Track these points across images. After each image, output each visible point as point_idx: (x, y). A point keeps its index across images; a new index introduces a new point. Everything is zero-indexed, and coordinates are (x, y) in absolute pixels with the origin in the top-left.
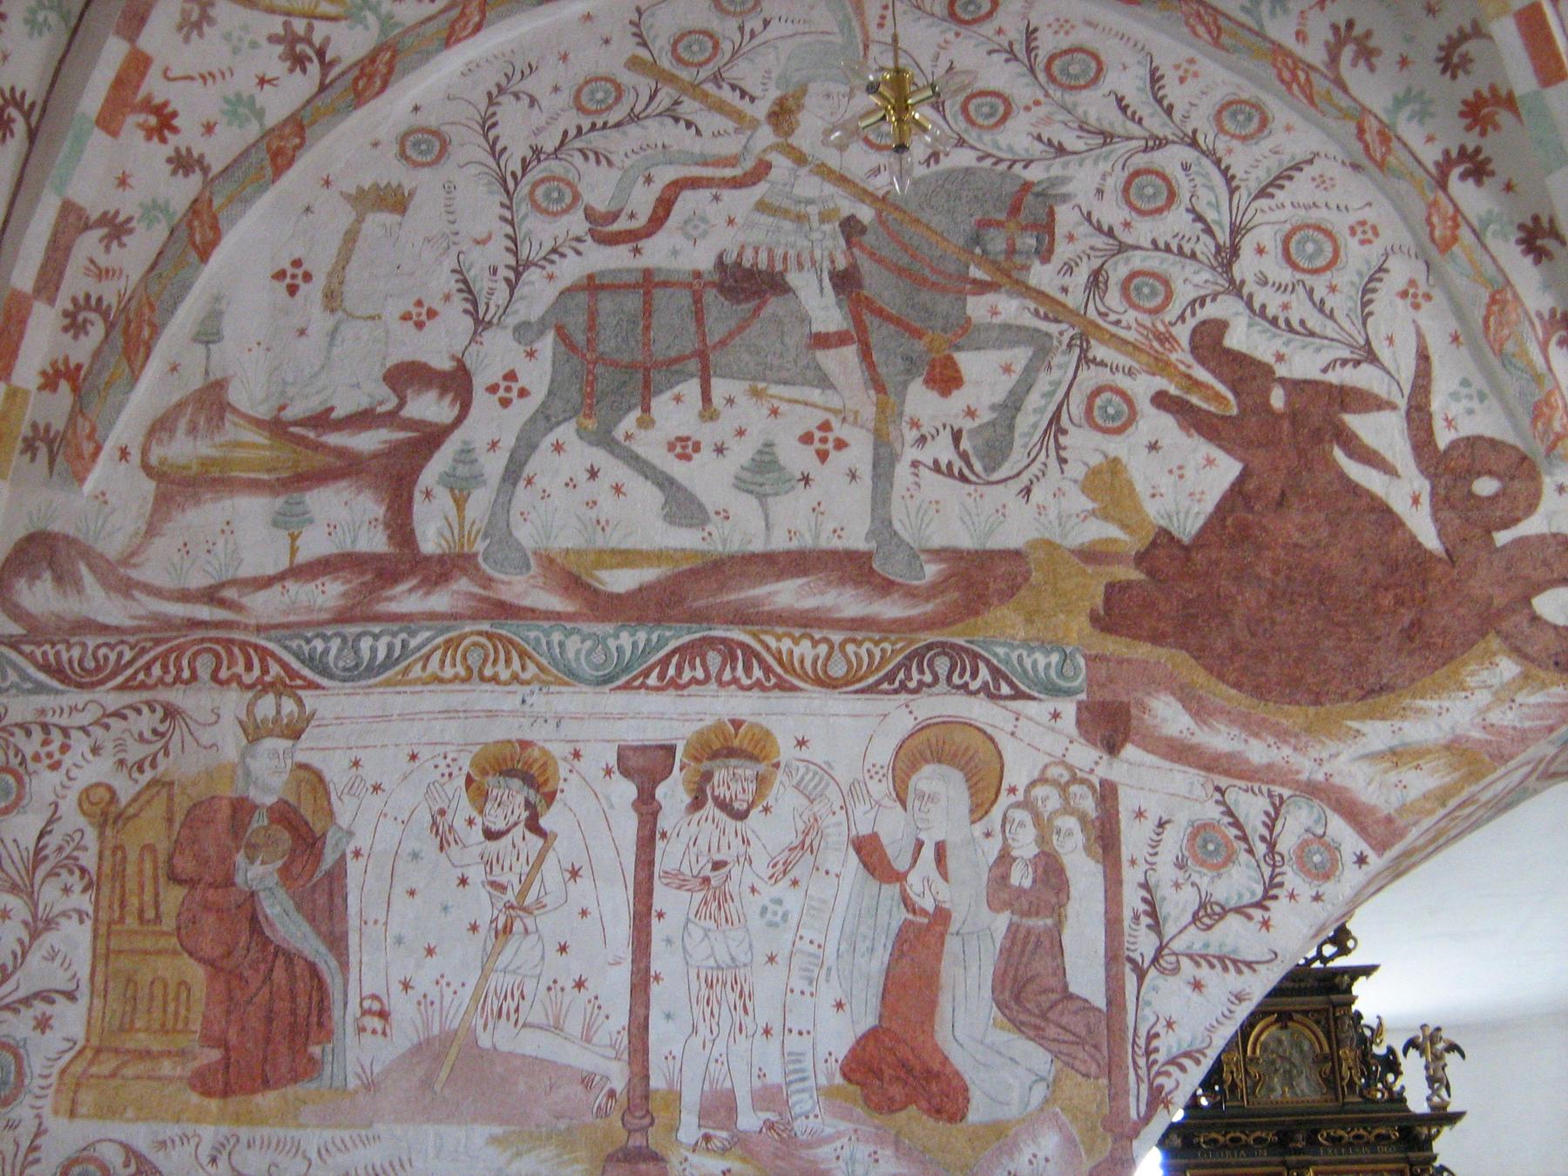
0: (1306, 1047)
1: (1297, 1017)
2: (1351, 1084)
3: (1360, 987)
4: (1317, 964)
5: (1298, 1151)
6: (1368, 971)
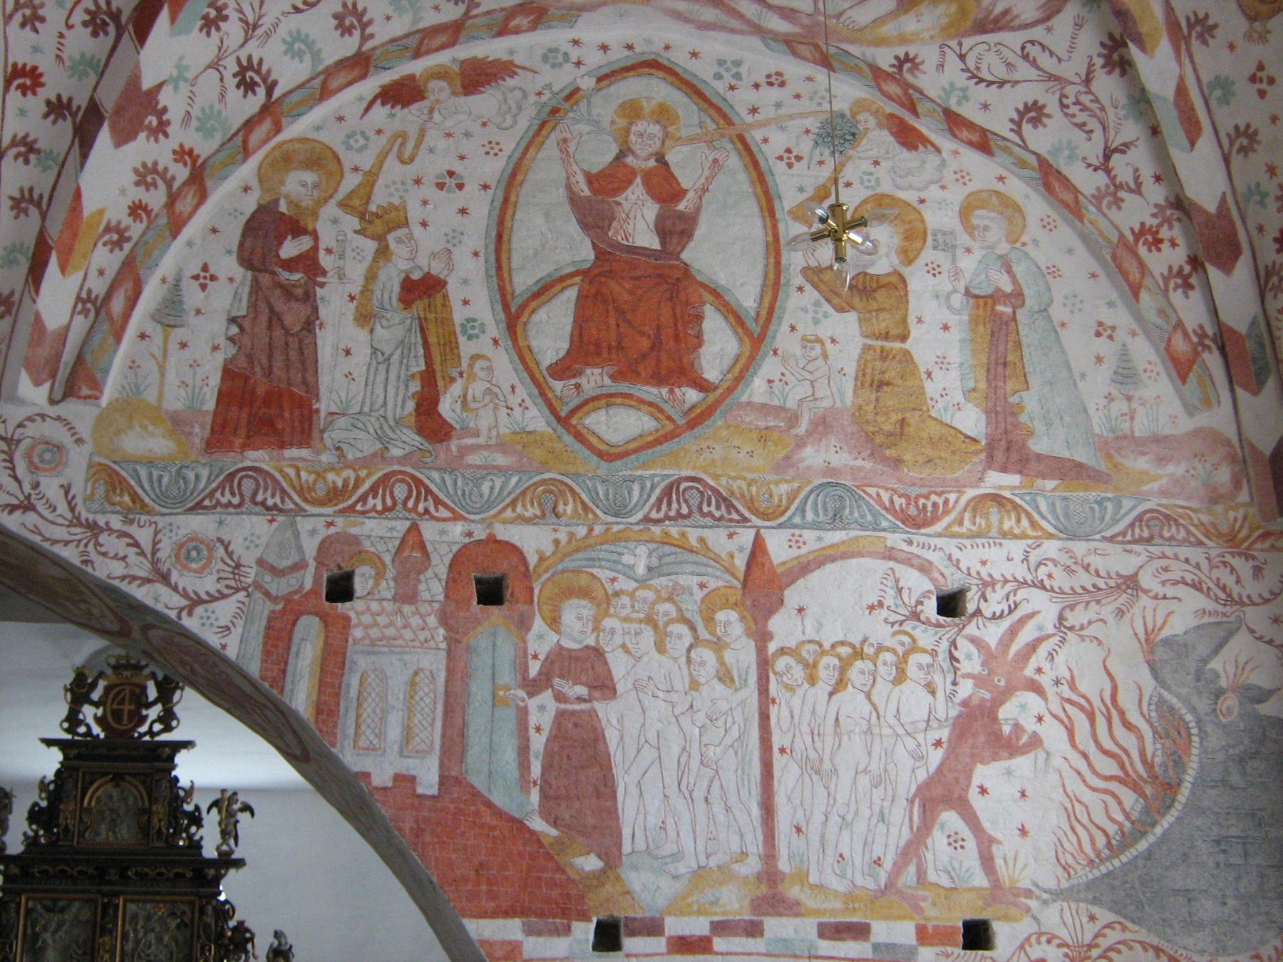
0: (131, 801)
1: (128, 778)
2: (159, 832)
3: (181, 758)
4: (147, 738)
5: (110, 883)
6: (188, 744)
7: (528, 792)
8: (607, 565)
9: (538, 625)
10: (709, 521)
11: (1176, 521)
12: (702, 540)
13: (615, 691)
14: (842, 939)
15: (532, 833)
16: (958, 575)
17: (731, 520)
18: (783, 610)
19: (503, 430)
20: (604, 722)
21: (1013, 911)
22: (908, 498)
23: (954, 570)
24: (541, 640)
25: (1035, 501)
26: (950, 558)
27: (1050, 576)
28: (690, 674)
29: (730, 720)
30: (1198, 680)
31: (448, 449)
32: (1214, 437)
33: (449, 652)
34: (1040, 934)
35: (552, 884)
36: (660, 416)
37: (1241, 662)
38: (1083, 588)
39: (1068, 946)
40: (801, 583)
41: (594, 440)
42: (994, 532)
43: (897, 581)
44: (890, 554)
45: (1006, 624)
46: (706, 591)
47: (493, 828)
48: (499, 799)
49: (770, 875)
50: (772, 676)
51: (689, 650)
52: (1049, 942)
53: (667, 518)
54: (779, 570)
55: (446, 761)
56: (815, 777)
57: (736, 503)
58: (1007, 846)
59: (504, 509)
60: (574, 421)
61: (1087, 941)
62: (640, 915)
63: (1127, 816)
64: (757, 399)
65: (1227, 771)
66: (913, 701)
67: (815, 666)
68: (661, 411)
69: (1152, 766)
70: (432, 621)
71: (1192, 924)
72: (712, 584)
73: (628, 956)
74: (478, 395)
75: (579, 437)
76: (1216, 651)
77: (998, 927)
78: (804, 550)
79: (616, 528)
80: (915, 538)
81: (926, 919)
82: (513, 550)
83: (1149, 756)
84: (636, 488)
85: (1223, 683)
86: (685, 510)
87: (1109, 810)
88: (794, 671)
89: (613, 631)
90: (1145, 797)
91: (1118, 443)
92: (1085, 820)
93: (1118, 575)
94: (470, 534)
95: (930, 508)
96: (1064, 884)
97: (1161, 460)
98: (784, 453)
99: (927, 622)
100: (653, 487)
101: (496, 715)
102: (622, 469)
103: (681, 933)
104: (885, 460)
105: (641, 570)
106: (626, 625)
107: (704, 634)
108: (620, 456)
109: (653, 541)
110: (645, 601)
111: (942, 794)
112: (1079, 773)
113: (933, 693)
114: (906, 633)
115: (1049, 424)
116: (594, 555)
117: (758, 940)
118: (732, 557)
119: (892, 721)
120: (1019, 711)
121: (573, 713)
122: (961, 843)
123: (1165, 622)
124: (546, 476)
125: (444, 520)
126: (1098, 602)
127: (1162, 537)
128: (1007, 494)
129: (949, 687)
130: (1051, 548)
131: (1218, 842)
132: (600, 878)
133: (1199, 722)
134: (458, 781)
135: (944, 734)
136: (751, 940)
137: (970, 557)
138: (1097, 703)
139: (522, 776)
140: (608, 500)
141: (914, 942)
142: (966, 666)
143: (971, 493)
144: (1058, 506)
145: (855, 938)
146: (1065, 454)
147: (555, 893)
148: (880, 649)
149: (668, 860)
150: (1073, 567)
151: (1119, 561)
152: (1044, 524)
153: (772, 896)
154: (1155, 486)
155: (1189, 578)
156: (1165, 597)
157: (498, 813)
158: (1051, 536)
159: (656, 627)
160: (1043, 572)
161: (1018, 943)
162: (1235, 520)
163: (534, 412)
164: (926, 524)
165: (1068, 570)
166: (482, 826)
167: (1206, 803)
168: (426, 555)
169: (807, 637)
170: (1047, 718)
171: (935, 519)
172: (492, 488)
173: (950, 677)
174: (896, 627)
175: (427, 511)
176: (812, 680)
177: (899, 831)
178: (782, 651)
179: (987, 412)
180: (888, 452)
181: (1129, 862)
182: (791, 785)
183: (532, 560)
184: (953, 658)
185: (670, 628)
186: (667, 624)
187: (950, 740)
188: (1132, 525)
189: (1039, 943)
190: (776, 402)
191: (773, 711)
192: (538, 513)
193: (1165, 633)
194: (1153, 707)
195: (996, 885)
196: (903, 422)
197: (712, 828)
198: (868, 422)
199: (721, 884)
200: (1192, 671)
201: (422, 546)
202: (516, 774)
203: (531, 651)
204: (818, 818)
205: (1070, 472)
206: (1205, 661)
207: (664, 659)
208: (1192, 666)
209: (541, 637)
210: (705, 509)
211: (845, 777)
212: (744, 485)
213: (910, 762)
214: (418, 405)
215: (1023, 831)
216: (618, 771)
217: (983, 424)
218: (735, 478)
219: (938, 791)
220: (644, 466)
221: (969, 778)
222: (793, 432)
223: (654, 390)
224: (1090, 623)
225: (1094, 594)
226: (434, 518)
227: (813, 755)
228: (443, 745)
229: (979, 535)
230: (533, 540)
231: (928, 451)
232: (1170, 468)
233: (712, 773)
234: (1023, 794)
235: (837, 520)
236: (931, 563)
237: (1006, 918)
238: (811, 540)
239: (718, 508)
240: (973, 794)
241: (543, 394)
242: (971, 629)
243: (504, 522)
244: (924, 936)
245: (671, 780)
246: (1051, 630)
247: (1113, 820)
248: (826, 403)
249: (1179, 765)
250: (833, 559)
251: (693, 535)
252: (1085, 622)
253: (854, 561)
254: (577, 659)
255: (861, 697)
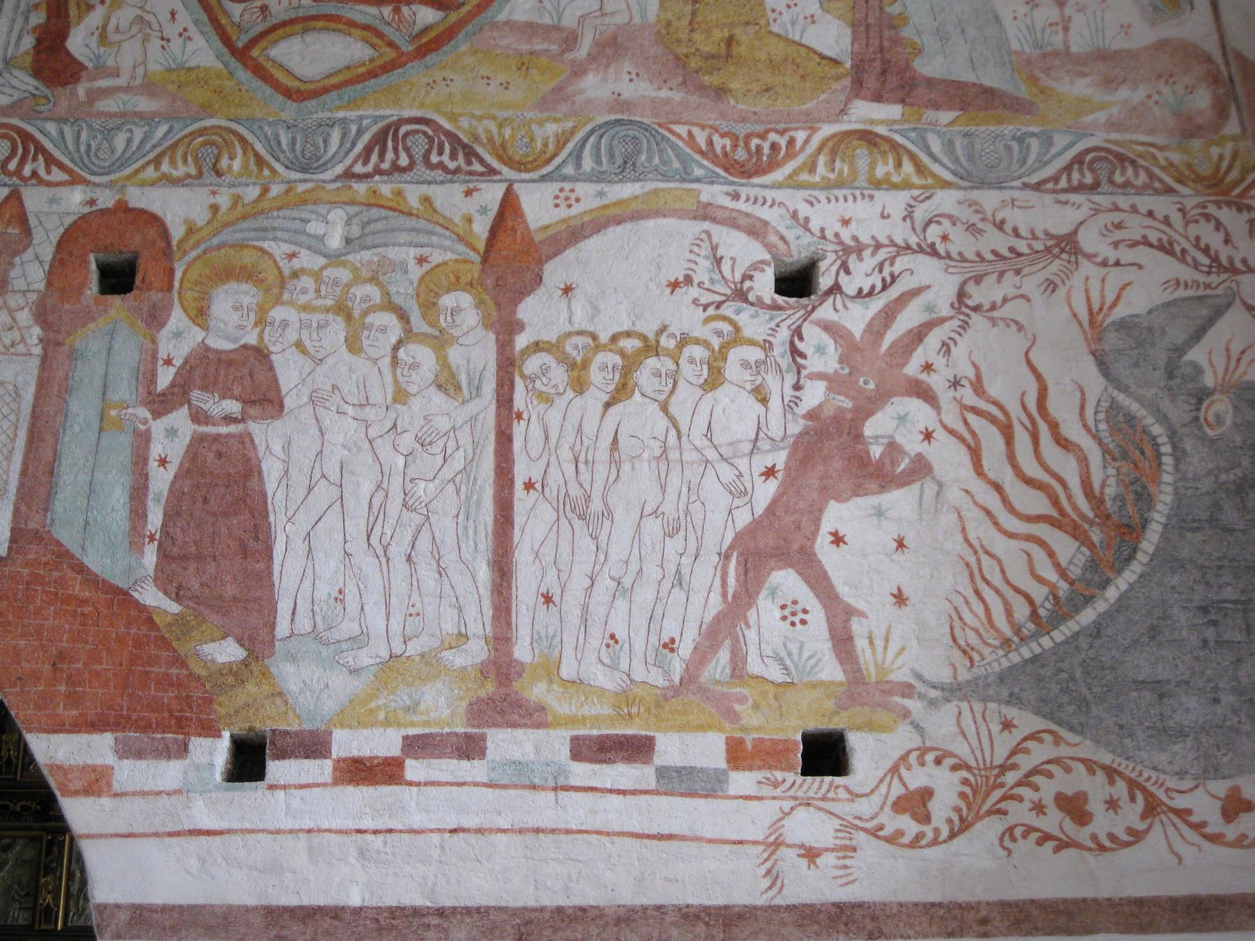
7: (141, 552)
8: (286, 236)
9: (177, 318)
10: (438, 174)
11: (1133, 162)
12: (427, 200)
13: (282, 406)
14: (610, 761)
15: (141, 608)
16: (807, 239)
17: (471, 173)
18: (541, 291)
19: (153, 67)
20: (261, 449)
21: (882, 716)
22: (735, 138)
23: (800, 231)
24: (179, 338)
25: (924, 139)
26: (795, 215)
27: (945, 238)
28: (396, 382)
29: (451, 445)
30: (1171, 375)
31: (73, 94)
32: (1187, 52)
33: (45, 360)
34: (923, 751)
35: (165, 682)
36: (375, 40)
37: (1236, 348)
38: (994, 253)
39: (968, 768)
40: (570, 253)
41: (280, 75)
42: (862, 180)
43: (714, 248)
44: (706, 213)
45: (877, 304)
46: (427, 267)
47: (84, 602)
48: (95, 561)
49: (501, 667)
50: (518, 380)
51: (396, 349)
52: (938, 762)
53: (378, 171)
54: (538, 238)
55: (23, 508)
56: (578, 524)
57: (480, 150)
58: (874, 616)
59: (143, 167)
60: (255, 53)
61: (998, 760)
62: (295, 728)
63: (1063, 573)
64: (520, 17)
65: (1217, 506)
66: (734, 412)
67: (585, 365)
68: (380, 35)
69: (1102, 501)
70: (25, 317)
71: (1164, 733)
72: (437, 257)
73: (272, 787)
74: (124, 25)
75: (260, 72)
76: (1198, 335)
77: (854, 740)
78: (577, 209)
79: (301, 188)
80: (744, 192)
81: (744, 729)
82: (154, 220)
83: (1097, 485)
84: (336, 135)
85: (1209, 381)
86: (404, 161)
87: (1033, 565)
88: (551, 374)
89: (285, 324)
90: (1091, 546)
91: (1046, 62)
92: (997, 580)
93: (1047, 233)
94: (92, 202)
95: (766, 151)
96: (964, 675)
97: (1109, 83)
98: (554, 83)
99: (759, 303)
100: (360, 132)
101: (104, 442)
102: (315, 111)
103: (355, 753)
104: (702, 89)
105: (335, 242)
106: (304, 316)
107: (419, 324)
108: (315, 94)
109: (353, 203)
110: (336, 282)
111: (775, 544)
112: (988, 513)
113: (764, 401)
114: (725, 318)
115: (942, 36)
116: (266, 223)
117: (476, 762)
118: (470, 221)
119: (700, 442)
120: (895, 424)
121: (217, 438)
122: (801, 616)
123: (1118, 297)
124: (208, 123)
125: (59, 184)
126: (1018, 272)
127: (1111, 182)
128: (882, 130)
129: (789, 392)
130: (946, 200)
131: (1204, 610)
132: (238, 673)
133: (1173, 435)
134: (38, 537)
135: (780, 459)
136: (464, 763)
137: (825, 215)
138: (1015, 411)
139: (133, 528)
140: (293, 150)
141: (723, 764)
142: (814, 363)
143: (827, 130)
144: (958, 144)
145: (629, 759)
146: (969, 77)
147: (169, 695)
148: (684, 341)
149: (344, 646)
150: (980, 225)
151: (1053, 216)
152: (936, 168)
153: (503, 696)
154: (1102, 116)
155: (1153, 237)
156: (1117, 264)
157: (92, 580)
158: (947, 185)
159: (349, 317)
160: (933, 233)
161: (888, 764)
162: (1221, 158)
163: (199, 42)
164: (760, 171)
165: (971, 228)
166: (68, 599)
167: (1185, 553)
168: (27, 231)
169: (576, 327)
170: (940, 434)
171: (773, 165)
172: (129, 141)
173: (790, 379)
174: (711, 311)
175: (34, 174)
176: (579, 386)
177: (705, 601)
178: (537, 347)
179: (854, 25)
180: (706, 79)
181: (1066, 642)
182: (539, 536)
183: (177, 232)
184: (795, 352)
185: (370, 318)
186: (365, 314)
187: (788, 468)
188: (1068, 169)
189: (922, 764)
190: (547, 20)
191: (518, 430)
192: (193, 171)
193: (1120, 312)
194: (1101, 416)
195: (856, 677)
196: (730, 41)
197: (415, 598)
198: (679, 41)
199: (424, 680)
200: (1162, 364)
201: (23, 220)
202: (125, 526)
203: (162, 354)
204: (579, 582)
205: (973, 99)
206: (1180, 350)
207: (360, 363)
208: (1160, 356)
209: (178, 335)
210: (434, 159)
211: (624, 521)
212: (492, 126)
213: (725, 500)
214: (39, 41)
215: (900, 598)
216: (277, 519)
217: (848, 40)
218: (481, 118)
219: (766, 541)
220: (349, 105)
221: (817, 523)
222: (569, 56)
223: (373, 10)
224: (1005, 300)
225: (1010, 261)
226: (41, 182)
227: (574, 491)
228: (21, 486)
229: (840, 184)
230: (179, 207)
231: (767, 78)
232: (1124, 93)
233: (418, 519)
234: (901, 544)
235: (627, 168)
236: (766, 223)
237: (870, 726)
238: (588, 197)
239: (453, 156)
240: (822, 546)
241: (214, 21)
242: (825, 312)
243: (143, 184)
244: (738, 755)
245: (356, 528)
246: (945, 311)
247: (1041, 580)
248: (621, 19)
249: (1144, 499)
250: (618, 221)
251: (413, 195)
252: (999, 299)
253: (651, 223)
254: (230, 363)
255: (654, 408)
